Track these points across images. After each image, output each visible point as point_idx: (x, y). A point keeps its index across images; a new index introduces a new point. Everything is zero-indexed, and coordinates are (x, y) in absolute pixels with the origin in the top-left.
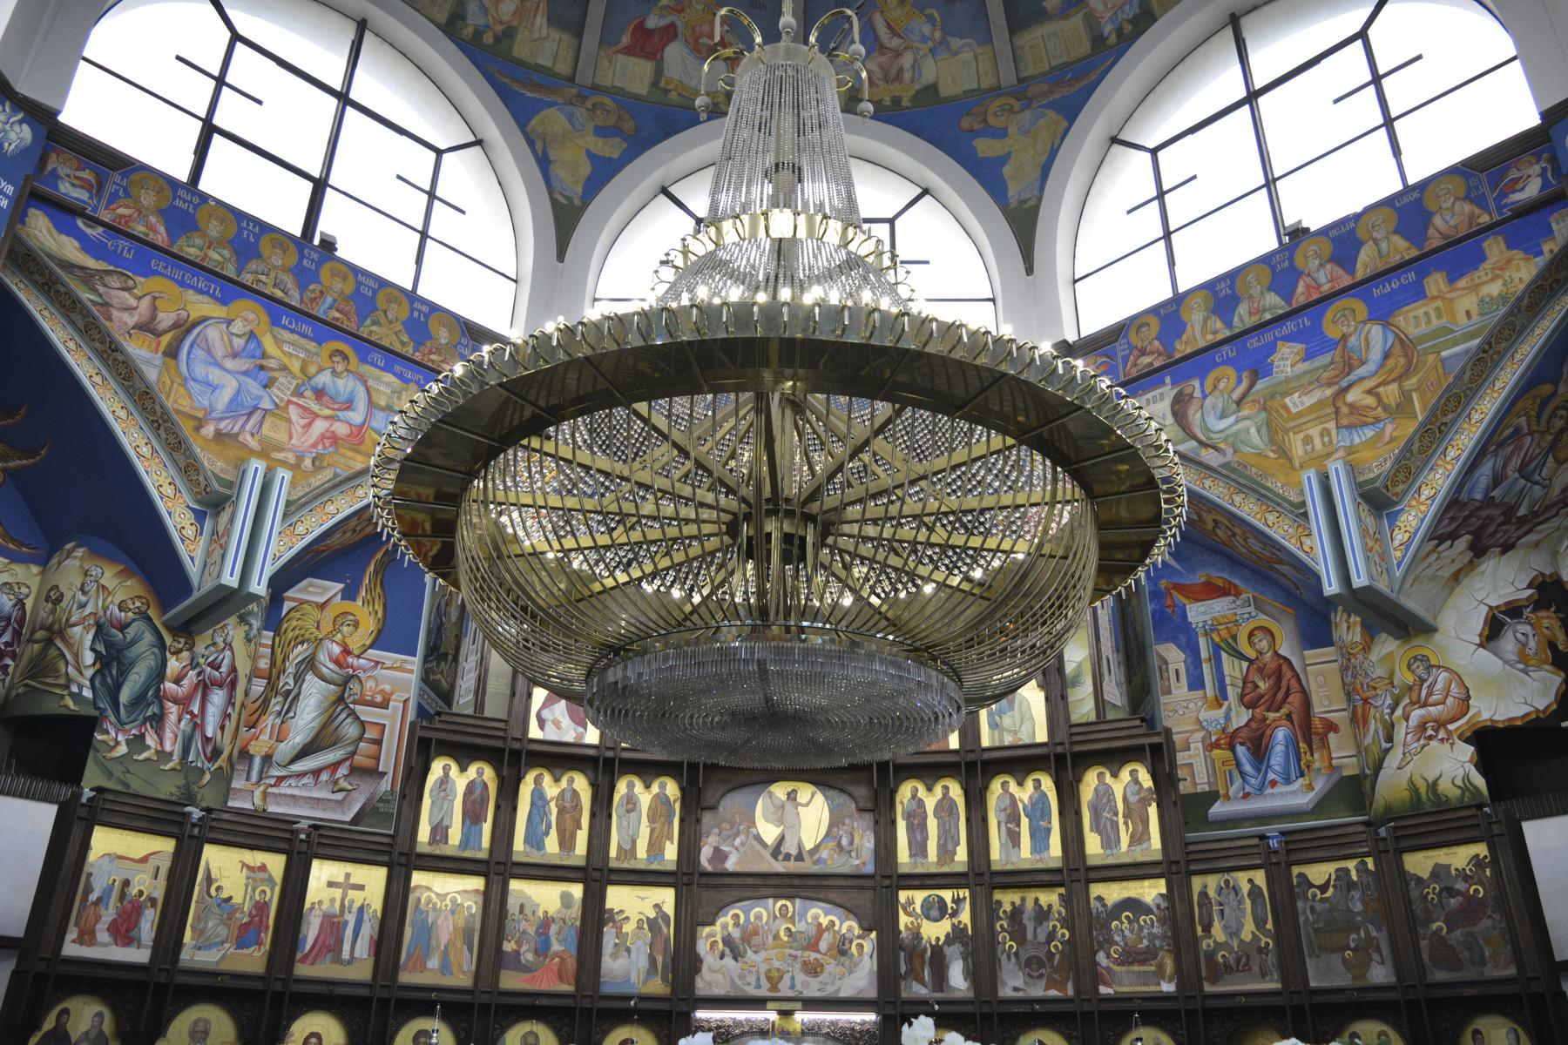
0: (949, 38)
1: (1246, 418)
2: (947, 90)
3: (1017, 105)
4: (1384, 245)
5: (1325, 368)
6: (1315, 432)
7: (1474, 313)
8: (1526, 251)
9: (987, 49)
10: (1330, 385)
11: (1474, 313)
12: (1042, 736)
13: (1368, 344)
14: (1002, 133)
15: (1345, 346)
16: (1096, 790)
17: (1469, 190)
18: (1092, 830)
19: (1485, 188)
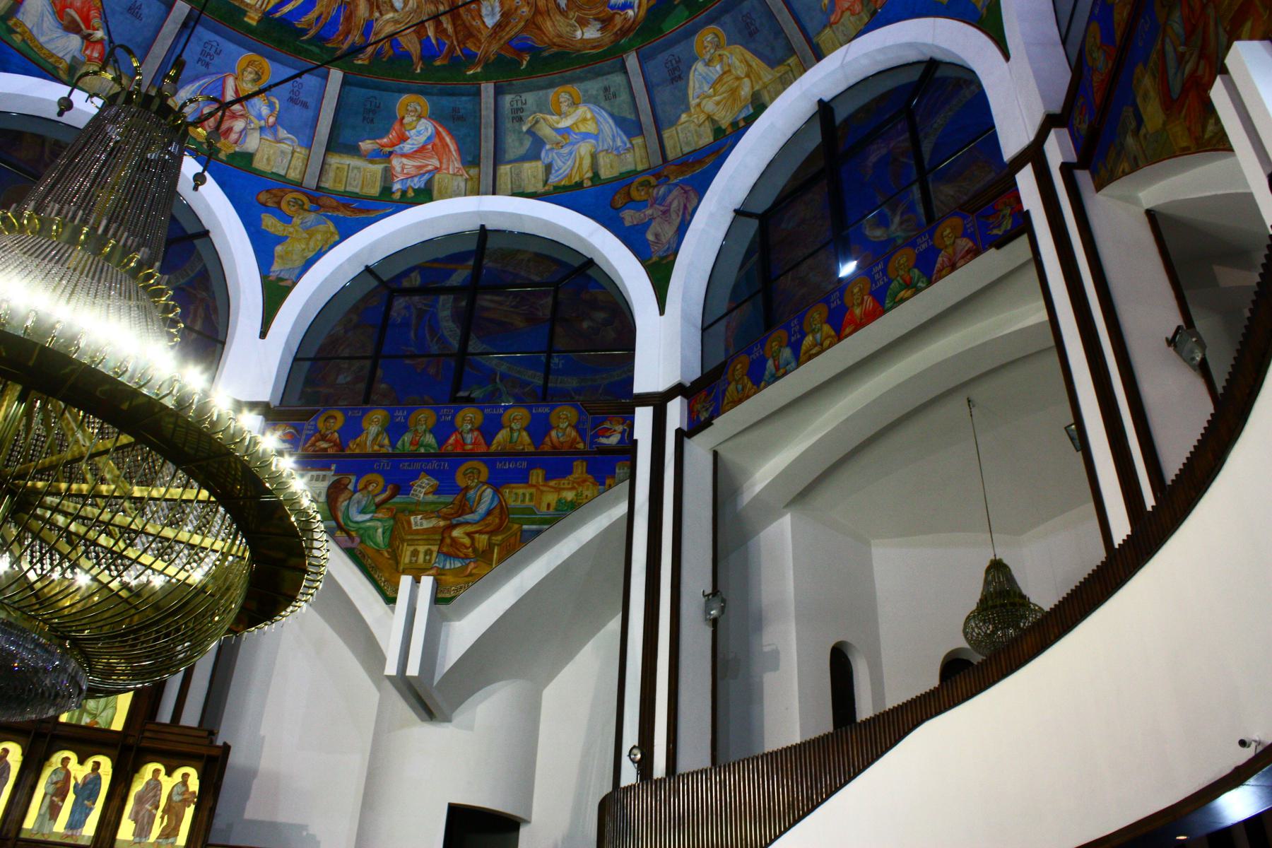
0: (279, 128)
1: (378, 520)
2: (260, 164)
3: (308, 205)
4: (516, 435)
5: (446, 505)
6: (422, 549)
7: (551, 509)
8: (596, 478)
9: (304, 151)
10: (445, 518)
12: (118, 725)
13: (480, 499)
14: (287, 219)
15: (465, 495)
16: (148, 783)
17: (578, 423)
18: (130, 818)
19: (588, 426)
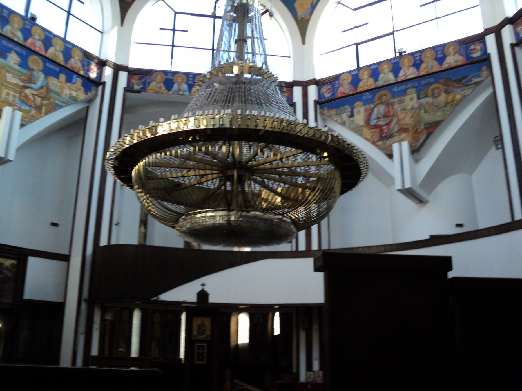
10: (23, 81)
11: (68, 96)
15: (32, 73)
19: (86, 63)
